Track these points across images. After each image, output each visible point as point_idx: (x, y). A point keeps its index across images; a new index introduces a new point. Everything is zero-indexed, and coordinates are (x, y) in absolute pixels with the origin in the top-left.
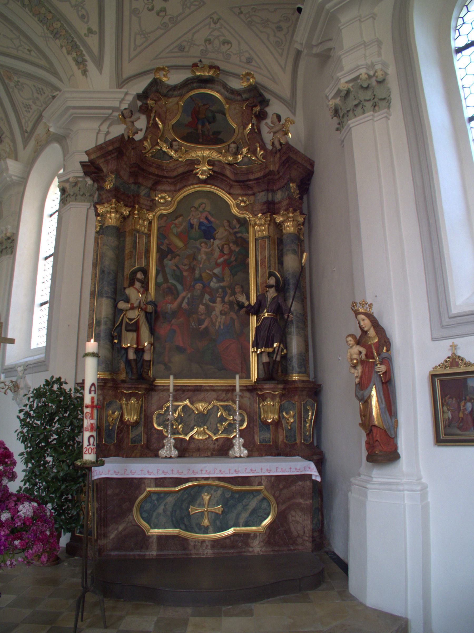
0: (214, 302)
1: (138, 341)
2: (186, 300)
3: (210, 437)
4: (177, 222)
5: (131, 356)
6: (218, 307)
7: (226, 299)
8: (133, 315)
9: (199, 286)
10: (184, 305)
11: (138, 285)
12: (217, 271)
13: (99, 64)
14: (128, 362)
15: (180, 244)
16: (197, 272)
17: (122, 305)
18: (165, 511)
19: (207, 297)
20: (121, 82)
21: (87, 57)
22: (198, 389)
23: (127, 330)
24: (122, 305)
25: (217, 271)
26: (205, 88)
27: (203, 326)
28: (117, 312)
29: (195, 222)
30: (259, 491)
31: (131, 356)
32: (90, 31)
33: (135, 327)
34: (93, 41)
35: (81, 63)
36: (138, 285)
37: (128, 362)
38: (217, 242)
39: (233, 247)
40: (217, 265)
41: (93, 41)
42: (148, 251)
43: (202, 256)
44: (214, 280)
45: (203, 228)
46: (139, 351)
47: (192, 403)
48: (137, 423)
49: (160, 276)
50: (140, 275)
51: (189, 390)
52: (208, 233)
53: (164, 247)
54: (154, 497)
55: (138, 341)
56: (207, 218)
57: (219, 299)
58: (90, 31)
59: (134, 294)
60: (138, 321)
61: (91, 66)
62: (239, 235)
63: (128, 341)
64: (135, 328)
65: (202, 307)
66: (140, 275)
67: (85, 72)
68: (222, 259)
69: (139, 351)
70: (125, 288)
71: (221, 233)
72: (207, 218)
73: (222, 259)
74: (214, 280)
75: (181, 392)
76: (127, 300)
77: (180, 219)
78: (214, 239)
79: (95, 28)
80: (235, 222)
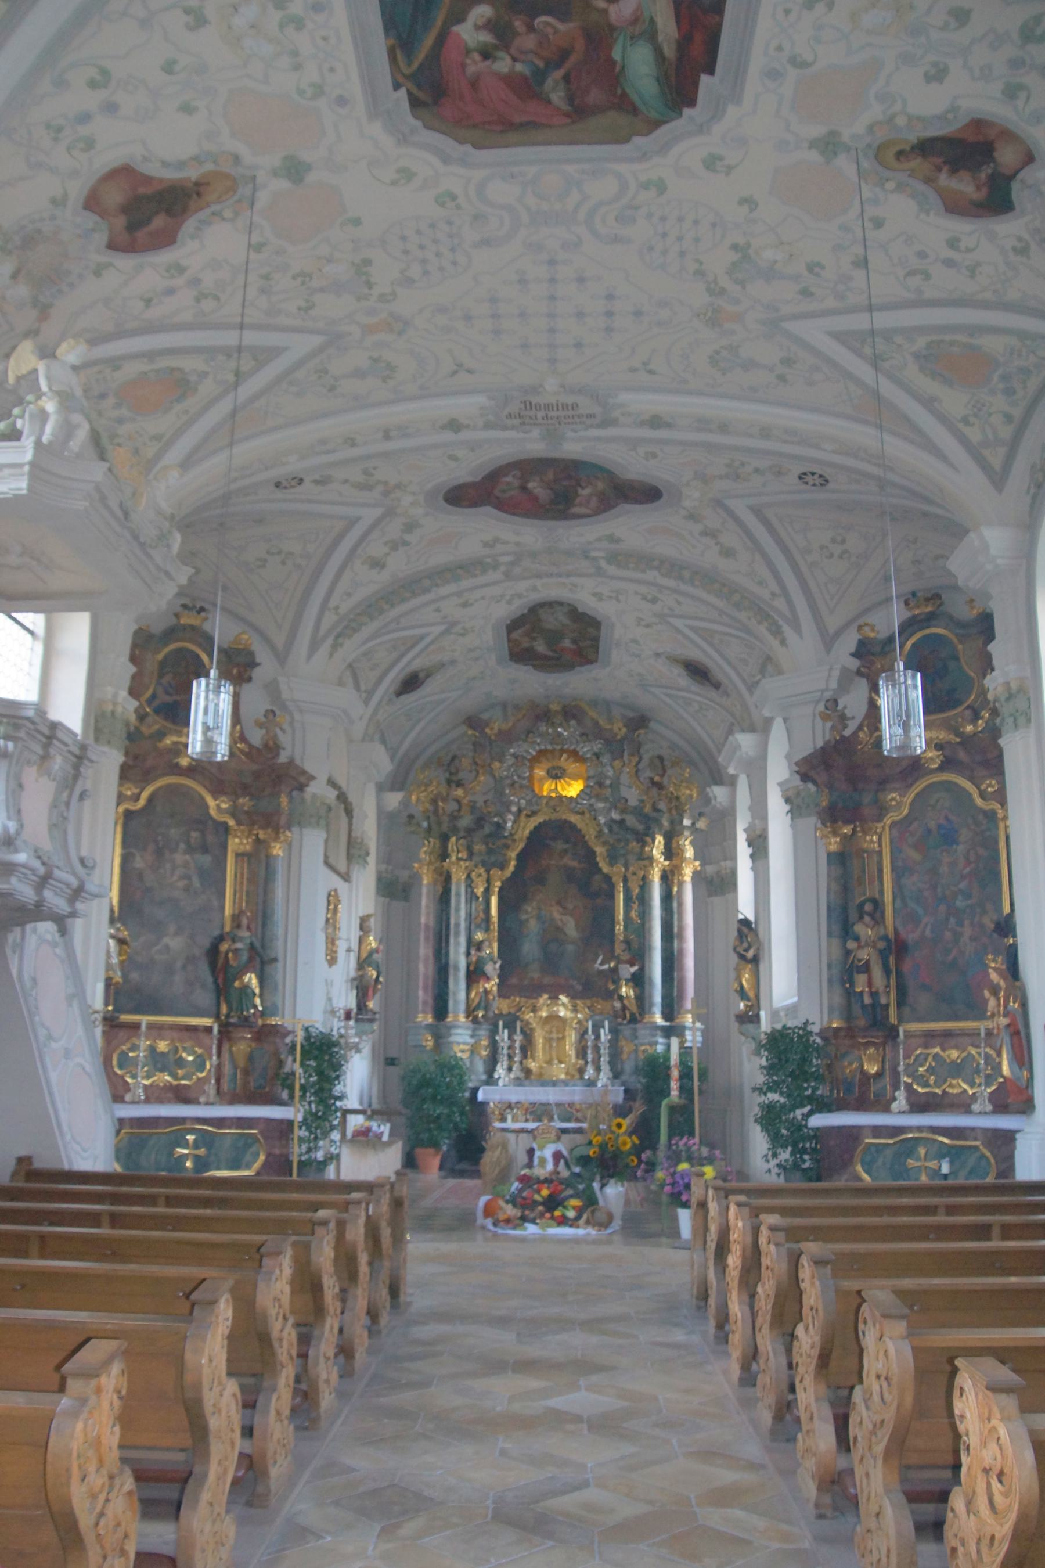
0: (962, 925)
1: (870, 984)
2: (929, 927)
3: (965, 1091)
4: (911, 828)
5: (867, 1000)
6: (967, 931)
7: (976, 920)
8: (864, 955)
9: (943, 908)
10: (928, 932)
11: (867, 919)
12: (963, 885)
13: (797, 628)
14: (864, 1007)
15: (916, 856)
16: (939, 890)
17: (851, 945)
18: (884, 1164)
19: (952, 920)
20: (829, 641)
21: (781, 622)
22: (948, 1034)
23: (858, 972)
24: (851, 945)
25: (963, 885)
26: (928, 627)
27: (950, 958)
28: (848, 953)
29: (932, 824)
30: (976, 1148)
31: (867, 1000)
32: (773, 594)
33: (866, 968)
34: (780, 603)
35: (777, 632)
36: (867, 919)
37: (864, 1007)
38: (961, 848)
39: (981, 851)
40: (963, 877)
41: (780, 603)
42: (880, 871)
43: (944, 869)
44: (960, 897)
45: (942, 832)
46: (874, 995)
47: (944, 1050)
48: (879, 1075)
49: (898, 902)
50: (868, 907)
51: (938, 1036)
52: (949, 838)
53: (900, 864)
54: (873, 1149)
55: (870, 984)
56: (946, 818)
57: (967, 922)
58: (773, 594)
59: (865, 930)
60: (867, 962)
61: (788, 631)
62: (988, 833)
63: (861, 983)
64: (866, 968)
65: (948, 934)
66: (868, 907)
67: (783, 642)
68: (968, 869)
69: (874, 995)
70: (853, 924)
71: (965, 835)
72: (946, 818)
73: (968, 869)
74: (960, 897)
75: (929, 1038)
76: (857, 939)
77: (915, 824)
78: (958, 844)
79: (777, 591)
80: (981, 817)
